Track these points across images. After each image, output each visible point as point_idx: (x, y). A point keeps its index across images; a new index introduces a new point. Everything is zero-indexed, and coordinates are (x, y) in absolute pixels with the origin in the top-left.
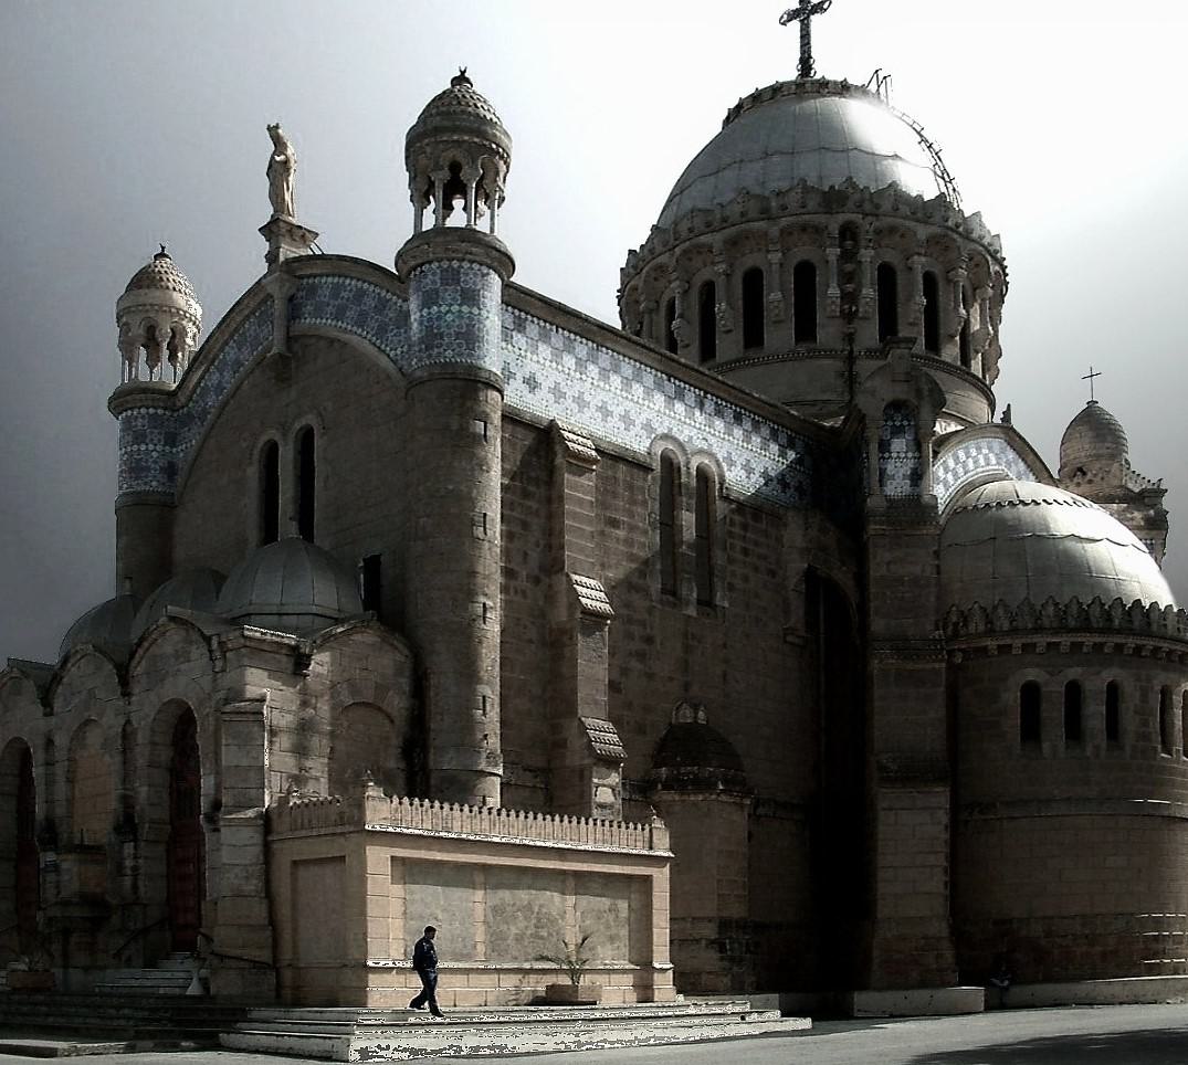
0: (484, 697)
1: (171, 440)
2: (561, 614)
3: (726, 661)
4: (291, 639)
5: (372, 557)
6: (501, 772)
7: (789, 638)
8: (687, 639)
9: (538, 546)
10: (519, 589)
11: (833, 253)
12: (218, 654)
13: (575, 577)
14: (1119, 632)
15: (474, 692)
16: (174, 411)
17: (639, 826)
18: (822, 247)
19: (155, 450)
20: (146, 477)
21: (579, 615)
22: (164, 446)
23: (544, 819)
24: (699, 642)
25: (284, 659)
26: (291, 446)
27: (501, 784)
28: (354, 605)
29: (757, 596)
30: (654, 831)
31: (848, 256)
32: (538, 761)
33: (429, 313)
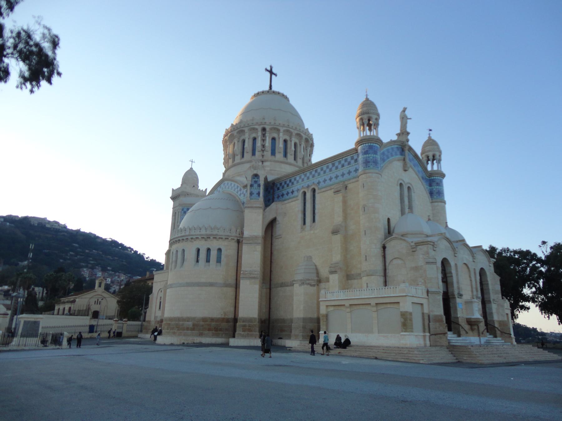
31: (264, 135)
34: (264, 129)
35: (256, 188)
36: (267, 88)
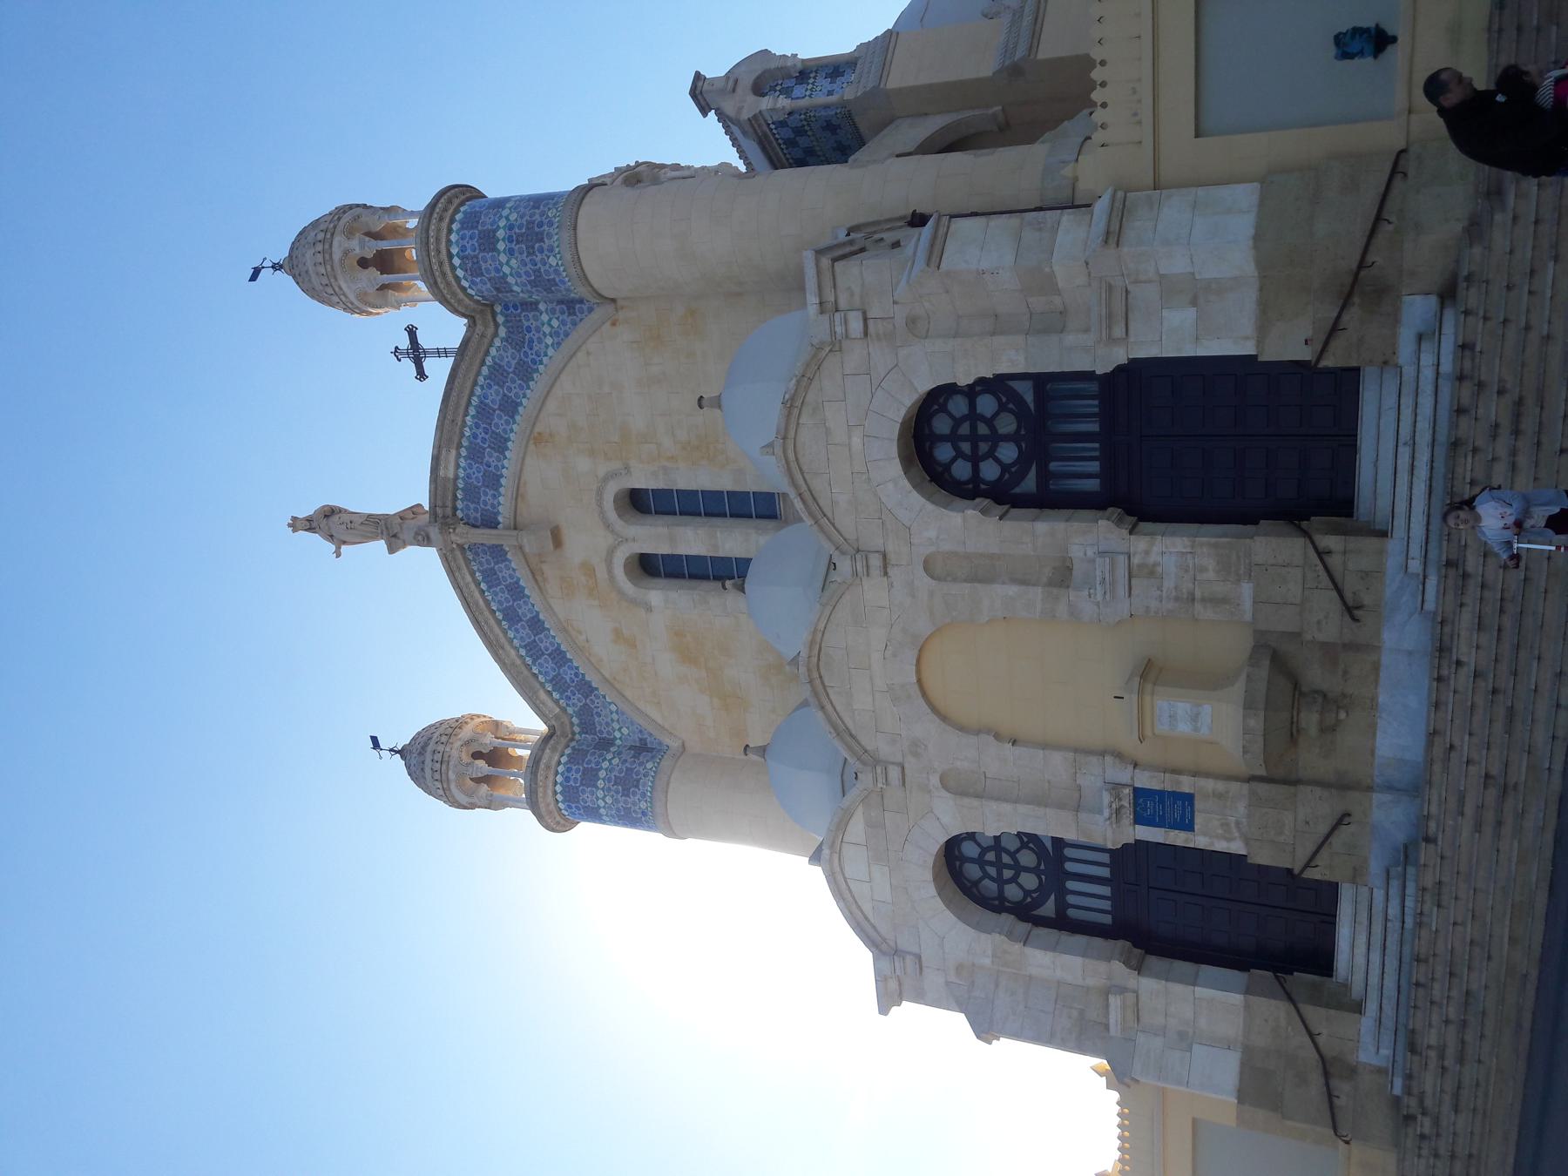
1: (605, 744)
19: (610, 761)
33: (503, 240)
35: (810, 86)
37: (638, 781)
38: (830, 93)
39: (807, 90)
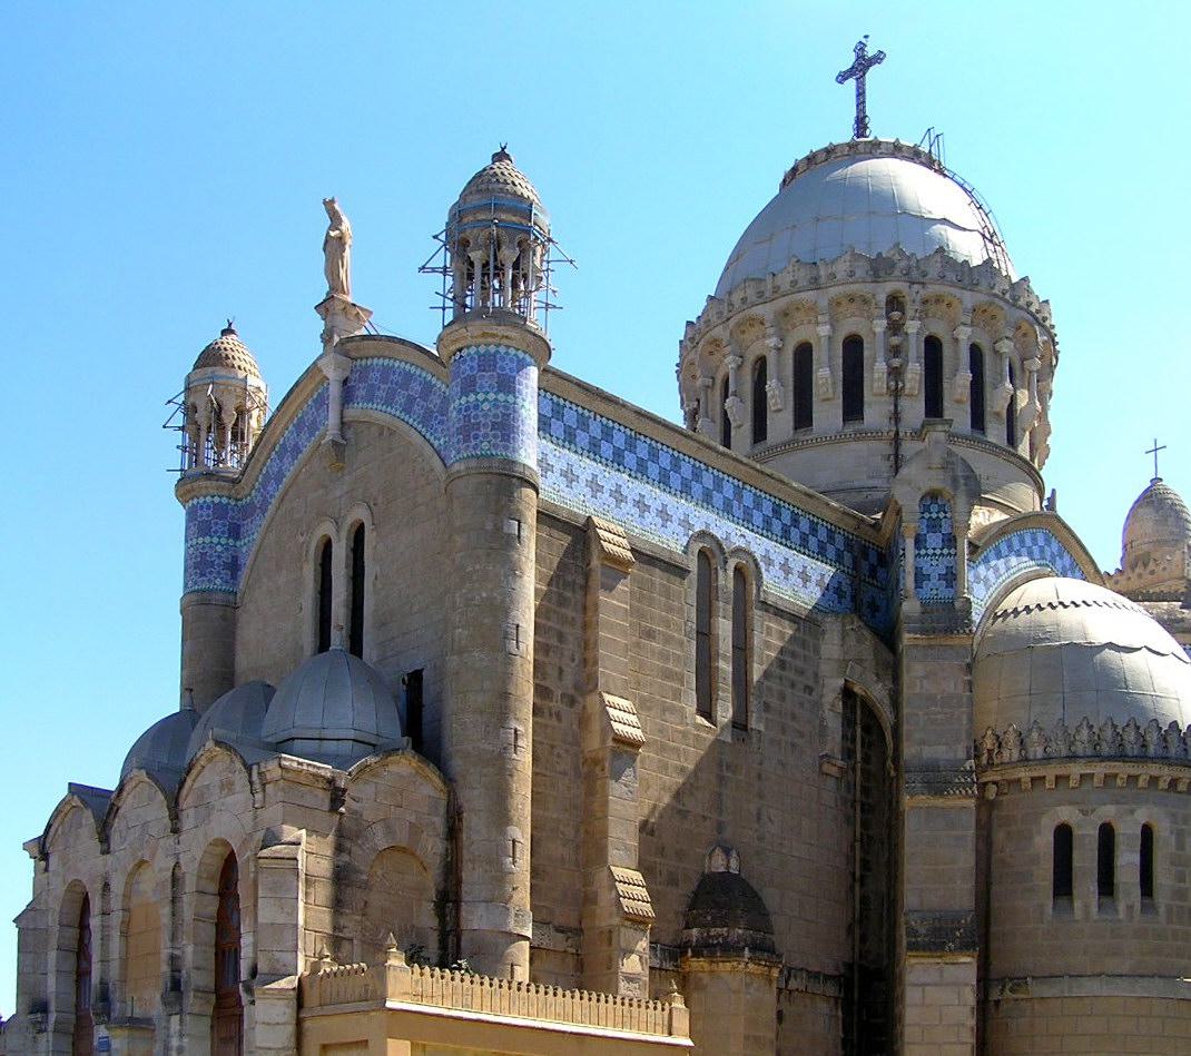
0: (514, 841)
1: (235, 532)
2: (593, 743)
3: (761, 796)
4: (326, 770)
5: (416, 671)
6: (529, 934)
7: (826, 768)
8: (721, 770)
9: (573, 660)
10: (553, 711)
11: (880, 325)
12: (257, 786)
13: (607, 697)
14: (1153, 759)
15: (503, 833)
16: (237, 500)
17: (659, 1006)
18: (871, 318)
19: (219, 543)
20: (211, 573)
21: (610, 743)
22: (228, 538)
23: (564, 996)
24: (734, 773)
25: (321, 793)
26: (343, 542)
27: (531, 947)
28: (392, 729)
29: (794, 717)
30: (674, 1012)
31: (895, 328)
32: (566, 917)
34: (894, 302)
36: (845, 134)
37: (205, 575)
38: (920, 578)
39: (934, 549)
